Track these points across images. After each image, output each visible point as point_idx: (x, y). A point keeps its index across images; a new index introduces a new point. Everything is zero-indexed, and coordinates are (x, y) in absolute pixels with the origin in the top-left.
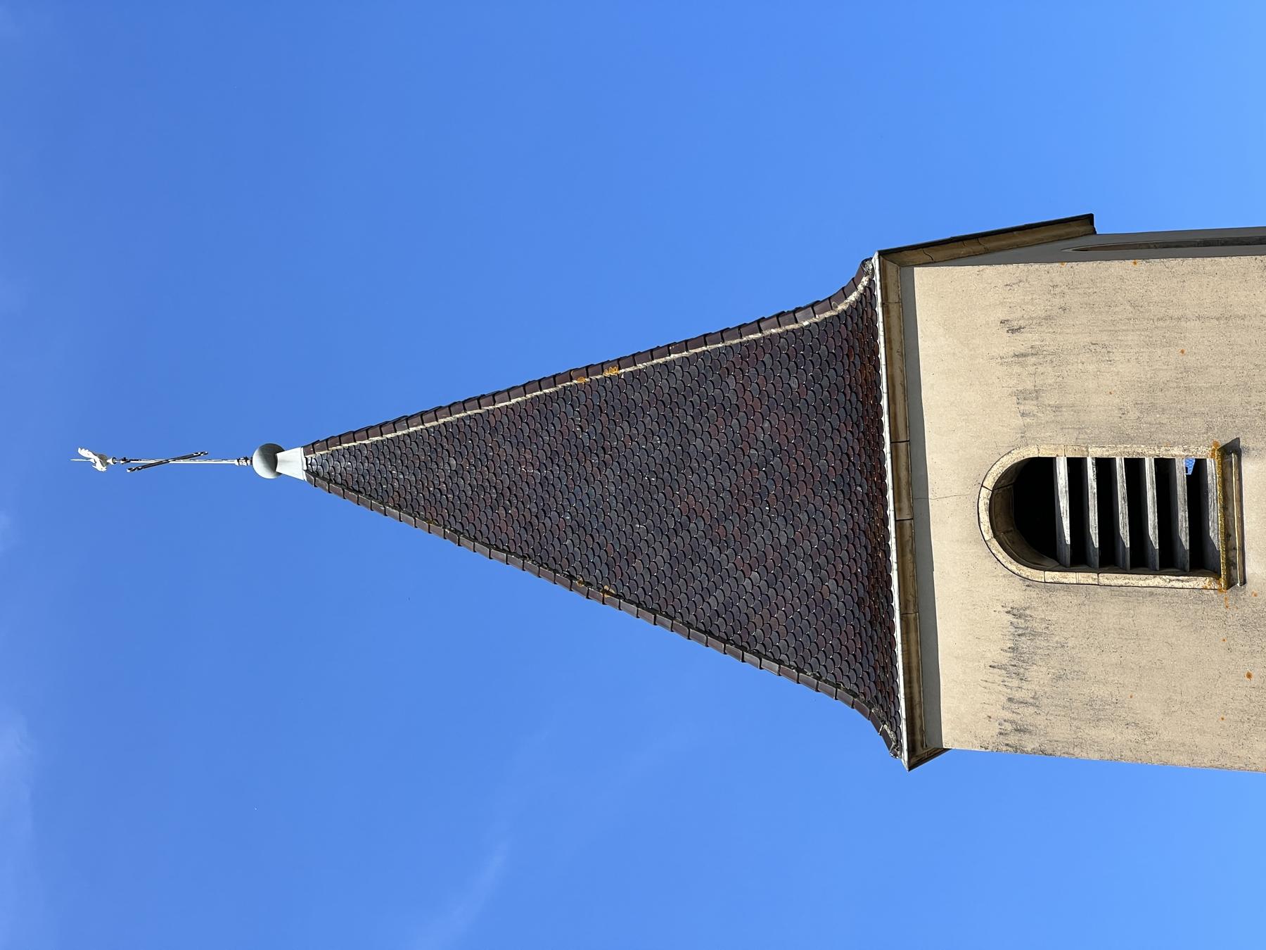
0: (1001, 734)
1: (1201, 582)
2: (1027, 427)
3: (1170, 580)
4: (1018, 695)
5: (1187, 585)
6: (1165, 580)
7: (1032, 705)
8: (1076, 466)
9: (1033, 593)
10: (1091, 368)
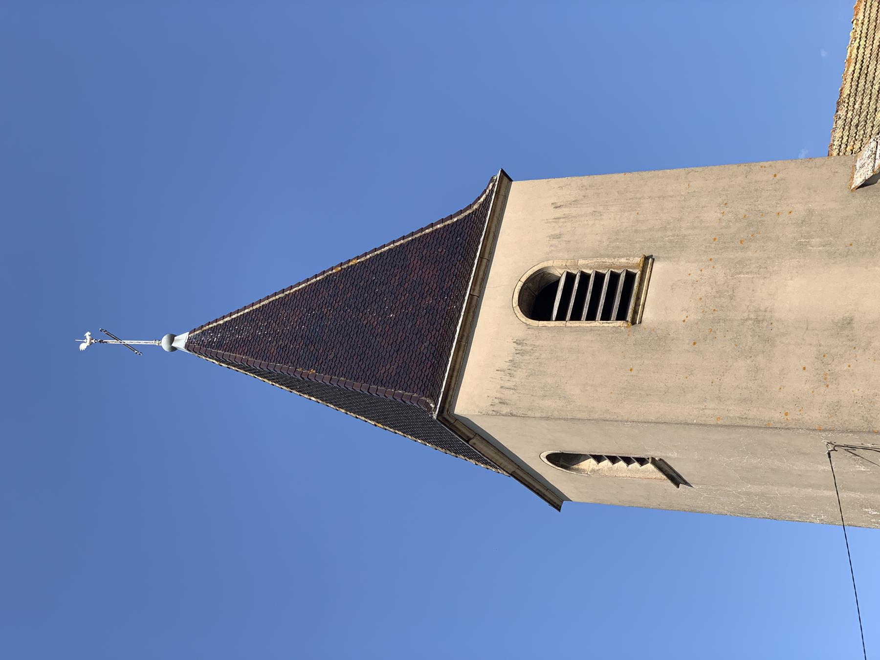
0: (492, 405)
2: (551, 251)
3: (603, 323)
4: (507, 385)
6: (600, 323)
7: (512, 389)
9: (530, 332)
10: (590, 223)
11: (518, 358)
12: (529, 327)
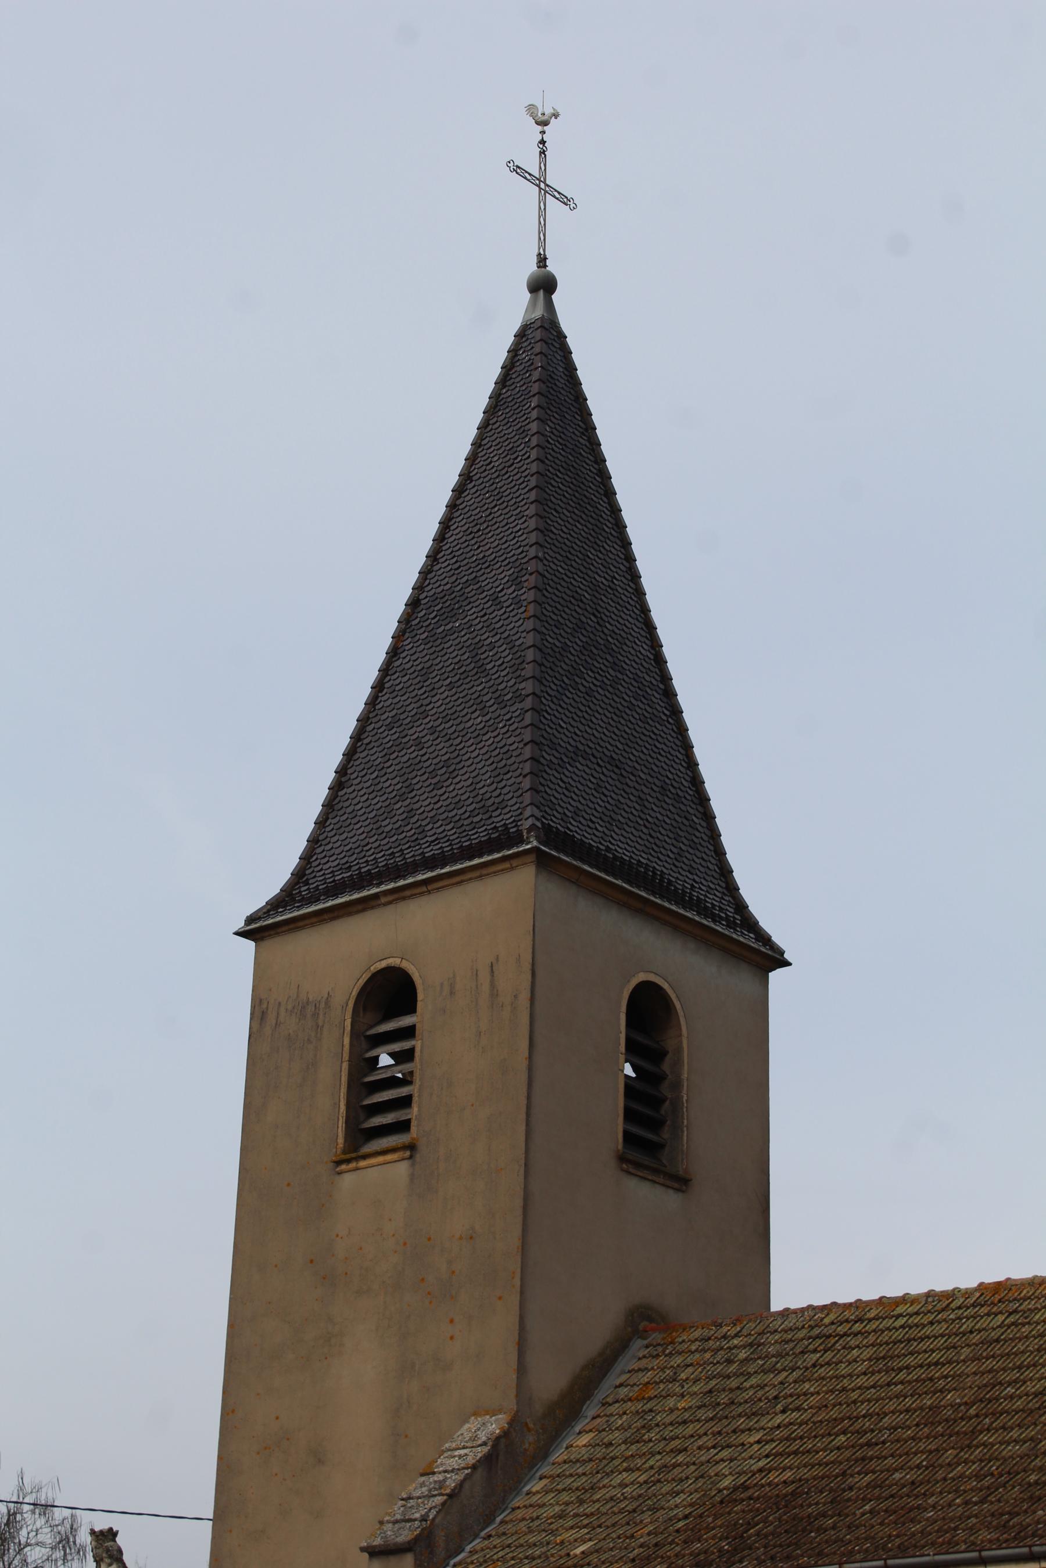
1: (341, 1140)
5: (340, 1130)
8: (409, 1032)
11: (310, 1009)
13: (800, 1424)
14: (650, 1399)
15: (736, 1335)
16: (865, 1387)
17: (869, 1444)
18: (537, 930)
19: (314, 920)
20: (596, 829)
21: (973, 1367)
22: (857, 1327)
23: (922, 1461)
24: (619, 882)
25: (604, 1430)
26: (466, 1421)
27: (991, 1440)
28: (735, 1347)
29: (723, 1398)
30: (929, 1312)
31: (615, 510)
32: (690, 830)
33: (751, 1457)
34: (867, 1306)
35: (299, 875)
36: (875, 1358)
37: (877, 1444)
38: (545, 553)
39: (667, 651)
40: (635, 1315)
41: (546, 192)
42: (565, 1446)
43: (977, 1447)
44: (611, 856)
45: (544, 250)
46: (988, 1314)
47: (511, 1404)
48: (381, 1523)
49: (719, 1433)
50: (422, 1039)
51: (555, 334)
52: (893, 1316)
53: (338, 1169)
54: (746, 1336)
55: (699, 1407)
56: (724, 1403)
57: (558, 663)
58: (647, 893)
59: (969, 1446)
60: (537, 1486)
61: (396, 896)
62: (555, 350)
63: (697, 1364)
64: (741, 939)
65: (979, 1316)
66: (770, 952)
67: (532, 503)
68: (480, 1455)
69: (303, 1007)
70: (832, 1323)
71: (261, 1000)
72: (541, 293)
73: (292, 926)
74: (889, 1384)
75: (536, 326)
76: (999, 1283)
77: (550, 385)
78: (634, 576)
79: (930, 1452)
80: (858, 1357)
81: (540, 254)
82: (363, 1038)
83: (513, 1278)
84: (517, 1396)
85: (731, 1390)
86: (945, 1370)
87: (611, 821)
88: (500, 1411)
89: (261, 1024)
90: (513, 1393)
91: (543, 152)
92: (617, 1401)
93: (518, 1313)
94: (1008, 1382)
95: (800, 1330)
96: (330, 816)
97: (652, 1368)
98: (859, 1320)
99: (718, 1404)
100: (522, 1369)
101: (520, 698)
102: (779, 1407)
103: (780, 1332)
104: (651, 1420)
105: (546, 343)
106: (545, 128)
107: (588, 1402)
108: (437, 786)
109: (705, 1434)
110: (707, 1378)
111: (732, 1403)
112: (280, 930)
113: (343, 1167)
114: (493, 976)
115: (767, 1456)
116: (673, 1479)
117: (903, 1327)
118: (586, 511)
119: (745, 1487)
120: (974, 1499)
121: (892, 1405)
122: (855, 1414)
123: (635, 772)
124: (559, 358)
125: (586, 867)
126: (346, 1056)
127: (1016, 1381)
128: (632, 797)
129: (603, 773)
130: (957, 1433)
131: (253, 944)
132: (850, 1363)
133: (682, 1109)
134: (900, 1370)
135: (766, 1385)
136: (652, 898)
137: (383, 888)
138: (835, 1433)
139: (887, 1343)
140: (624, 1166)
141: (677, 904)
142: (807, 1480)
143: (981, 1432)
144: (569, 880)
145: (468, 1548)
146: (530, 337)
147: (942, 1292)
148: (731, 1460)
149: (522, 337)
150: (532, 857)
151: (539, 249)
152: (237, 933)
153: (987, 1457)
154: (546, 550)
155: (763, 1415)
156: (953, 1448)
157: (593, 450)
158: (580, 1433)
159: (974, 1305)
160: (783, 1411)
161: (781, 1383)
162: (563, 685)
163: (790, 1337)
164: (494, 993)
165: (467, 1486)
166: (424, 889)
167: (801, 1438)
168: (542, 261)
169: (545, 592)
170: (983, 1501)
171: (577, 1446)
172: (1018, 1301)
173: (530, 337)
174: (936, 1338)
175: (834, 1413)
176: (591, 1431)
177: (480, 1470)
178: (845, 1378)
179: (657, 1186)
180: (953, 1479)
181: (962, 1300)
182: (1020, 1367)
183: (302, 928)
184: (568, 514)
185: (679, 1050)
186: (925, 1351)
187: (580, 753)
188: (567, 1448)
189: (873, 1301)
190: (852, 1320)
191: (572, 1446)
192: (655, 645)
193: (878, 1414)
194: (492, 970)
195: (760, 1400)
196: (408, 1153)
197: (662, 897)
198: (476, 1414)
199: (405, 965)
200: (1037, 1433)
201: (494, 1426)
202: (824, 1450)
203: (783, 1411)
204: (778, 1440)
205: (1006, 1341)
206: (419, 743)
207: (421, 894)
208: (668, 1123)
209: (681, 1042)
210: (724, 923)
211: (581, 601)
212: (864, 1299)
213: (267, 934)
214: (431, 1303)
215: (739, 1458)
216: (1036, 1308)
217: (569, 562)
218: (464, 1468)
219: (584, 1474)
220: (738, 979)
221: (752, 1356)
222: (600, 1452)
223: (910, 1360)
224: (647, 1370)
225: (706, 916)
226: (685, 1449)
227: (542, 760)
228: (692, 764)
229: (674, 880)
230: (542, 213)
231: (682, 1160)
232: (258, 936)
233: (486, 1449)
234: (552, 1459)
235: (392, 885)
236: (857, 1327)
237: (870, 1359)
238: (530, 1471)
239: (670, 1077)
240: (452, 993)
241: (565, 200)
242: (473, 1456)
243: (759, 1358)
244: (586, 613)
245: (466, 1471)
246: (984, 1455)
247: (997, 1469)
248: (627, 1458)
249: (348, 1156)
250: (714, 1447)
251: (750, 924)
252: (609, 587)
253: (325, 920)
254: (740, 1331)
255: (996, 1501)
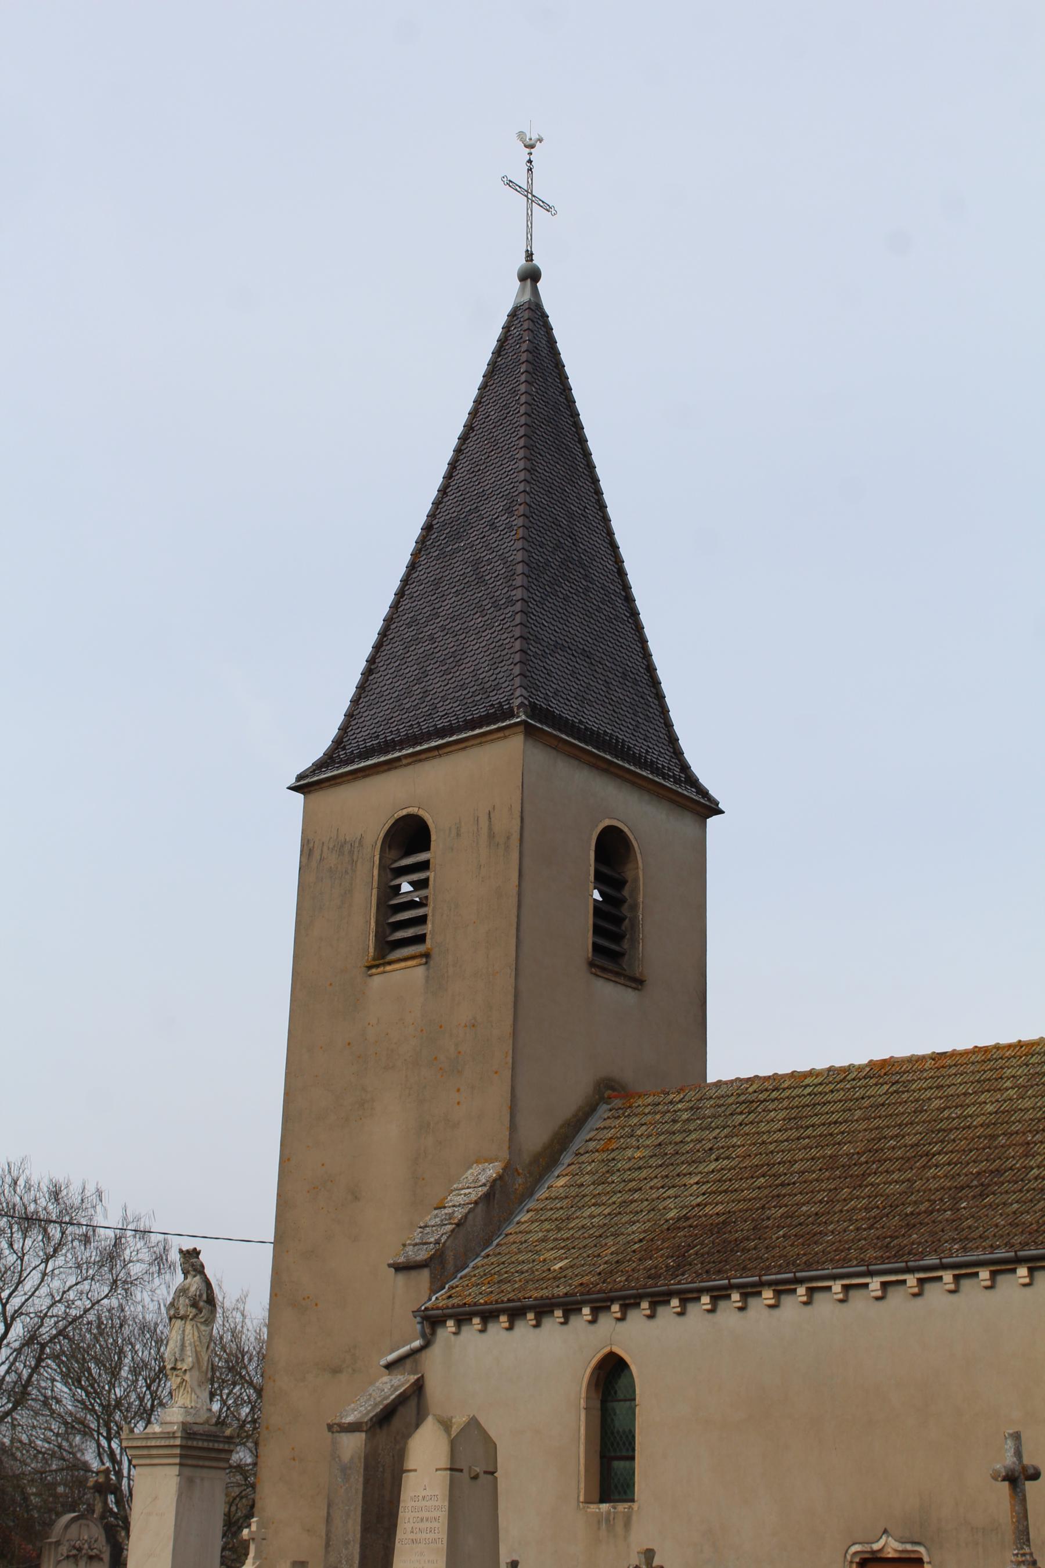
1: (371, 950)
4: (325, 848)
8: (425, 866)
11: (347, 848)
12: (374, 847)
13: (730, 1170)
14: (613, 1150)
15: (680, 1101)
16: (780, 1141)
17: (782, 1185)
18: (524, 786)
19: (350, 777)
20: (572, 706)
21: (864, 1125)
22: (774, 1094)
23: (824, 1198)
24: (589, 748)
25: (577, 1174)
26: (470, 1167)
27: (877, 1181)
28: (679, 1110)
29: (670, 1150)
30: (830, 1082)
31: (587, 454)
32: (645, 706)
33: (691, 1195)
34: (782, 1078)
35: (338, 743)
36: (788, 1118)
37: (789, 1185)
38: (531, 488)
39: (628, 566)
40: (602, 1085)
41: (532, 201)
42: (546, 1186)
43: (867, 1186)
44: (583, 727)
45: (531, 248)
46: (876, 1084)
47: (505, 1154)
48: (404, 1245)
49: (667, 1176)
50: (434, 871)
51: (540, 314)
52: (802, 1086)
53: (369, 972)
54: (688, 1102)
55: (651, 1157)
56: (670, 1154)
57: (542, 575)
58: (612, 757)
59: (860, 1186)
60: (524, 1217)
61: (414, 759)
62: (539, 326)
63: (650, 1123)
64: (685, 793)
65: (869, 1085)
66: (707, 803)
67: (521, 448)
68: (480, 1193)
69: (342, 846)
70: (755, 1092)
71: (308, 841)
72: (529, 281)
73: (332, 782)
74: (798, 1139)
75: (524, 307)
76: (884, 1061)
77: (535, 355)
78: (602, 507)
79: (830, 1190)
80: (775, 1117)
81: (527, 251)
82: (388, 870)
83: (506, 1057)
84: (509, 1148)
85: (676, 1143)
86: (843, 1127)
87: (583, 700)
88: (496, 1160)
89: (308, 859)
90: (506, 1145)
91: (530, 170)
92: (587, 1152)
93: (510, 1084)
94: (891, 1136)
95: (729, 1097)
96: (363, 696)
97: (615, 1127)
98: (776, 1089)
99: (666, 1154)
100: (513, 1127)
101: (511, 602)
102: (713, 1156)
103: (714, 1099)
104: (613, 1166)
105: (532, 321)
106: (532, 150)
107: (565, 1153)
108: (446, 672)
109: (656, 1177)
110: (657, 1134)
111: (677, 1153)
112: (323, 785)
113: (374, 971)
114: (490, 821)
115: (704, 1194)
116: (631, 1212)
117: (809, 1094)
118: (564, 455)
119: (686, 1218)
120: (863, 1226)
121: (801, 1155)
122: (772, 1161)
123: (603, 662)
124: (543, 333)
125: (564, 736)
126: (375, 884)
127: (896, 1136)
128: (599, 681)
129: (577, 662)
130: (851, 1176)
131: (302, 796)
132: (768, 1123)
133: (639, 926)
134: (807, 1127)
135: (703, 1139)
136: (615, 760)
137: (404, 752)
138: (757, 1176)
139: (797, 1107)
140: (593, 970)
141: (635, 765)
142: (735, 1212)
143: (870, 1175)
144: (550, 746)
145: (471, 1265)
146: (519, 316)
147: (840, 1067)
148: (676, 1197)
149: (514, 317)
150: (522, 728)
151: (527, 246)
152: (289, 788)
153: (874, 1193)
154: (532, 486)
155: (701, 1163)
156: (848, 1187)
157: (570, 406)
158: (558, 1176)
159: (865, 1078)
160: (717, 1160)
161: (715, 1138)
162: (546, 593)
163: (722, 1102)
164: (491, 835)
165: (470, 1217)
166: (436, 753)
167: (730, 1180)
168: (529, 256)
169: (531, 519)
170: (870, 1228)
171: (556, 1187)
172: (899, 1074)
173: (519, 316)
174: (836, 1103)
175: (756, 1161)
176: (567, 1175)
177: (480, 1205)
178: (764, 1134)
179: (619, 986)
180: (848, 1211)
181: (856, 1073)
182: (900, 1125)
183: (340, 784)
184: (550, 457)
185: (636, 879)
186: (827, 1113)
187: (559, 646)
188: (548, 1188)
189: (787, 1074)
190: (770, 1089)
191: (552, 1186)
192: (618, 561)
193: (790, 1161)
194: (490, 817)
195: (698, 1151)
196: (424, 960)
197: (623, 760)
198: (477, 1162)
199: (421, 813)
200: (912, 1176)
201: (492, 1171)
202: (748, 1189)
203: (717, 1160)
204: (712, 1181)
205: (890, 1105)
206: (432, 639)
207: (434, 757)
208: (628, 936)
209: (637, 874)
210: (672, 780)
211: (560, 526)
212: (780, 1072)
213: (312, 789)
214: (442, 1076)
215: (682, 1195)
216: (913, 1080)
217: (550, 495)
218: (468, 1204)
219: (561, 1208)
220: (681, 824)
221: (692, 1117)
222: (574, 1191)
223: (815, 1120)
224: (610, 1128)
225: (658, 775)
226: (640, 1189)
227: (529, 651)
228: (647, 655)
229: (632, 746)
230: (530, 217)
231: (638, 967)
232: (306, 790)
233: (485, 1189)
234: (536, 1196)
235: (411, 750)
236: (774, 1094)
237: (784, 1119)
238: (519, 1206)
239: (629, 900)
240: (458, 835)
241: (548, 208)
242: (475, 1194)
243: (698, 1119)
244: (564, 536)
245: (470, 1206)
246: (871, 1192)
247: (881, 1203)
248: (594, 1196)
249: (377, 962)
250: (662, 1187)
251: (692, 781)
252: (582, 515)
253: (358, 777)
254: (683, 1098)
255: (880, 1228)
